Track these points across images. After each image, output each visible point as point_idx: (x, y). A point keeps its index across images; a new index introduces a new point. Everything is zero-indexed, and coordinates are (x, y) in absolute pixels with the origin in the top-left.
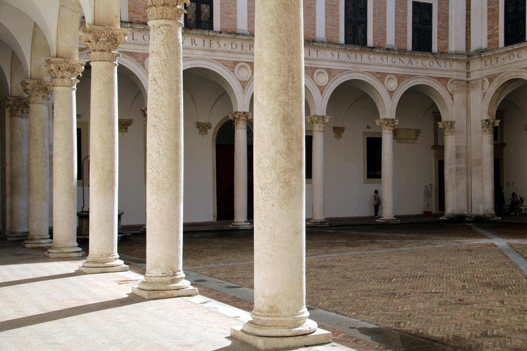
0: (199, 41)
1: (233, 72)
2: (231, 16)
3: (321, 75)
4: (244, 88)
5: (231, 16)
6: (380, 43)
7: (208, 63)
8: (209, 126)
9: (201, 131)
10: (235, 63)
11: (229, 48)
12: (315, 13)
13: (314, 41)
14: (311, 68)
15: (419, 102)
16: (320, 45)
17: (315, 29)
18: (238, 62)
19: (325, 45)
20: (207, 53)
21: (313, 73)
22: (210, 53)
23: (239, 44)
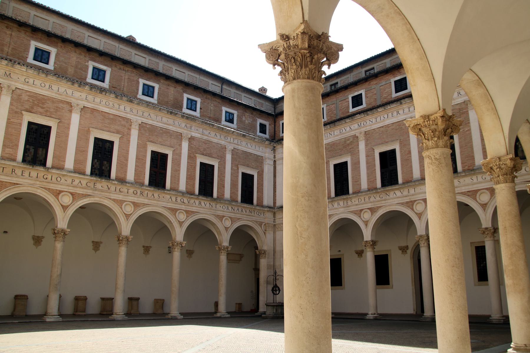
0: (341, 203)
1: (360, 216)
2: (358, 183)
3: (418, 205)
4: (366, 225)
5: (358, 183)
6: (469, 167)
7: (346, 214)
8: (407, 247)
9: (403, 252)
10: (361, 210)
11: (357, 202)
12: (411, 162)
13: (411, 181)
14: (411, 201)
15: (395, 222)
16: (413, 184)
17: (412, 173)
18: (363, 210)
19: (417, 183)
20: (345, 209)
21: (413, 205)
22: (347, 208)
23: (362, 198)
